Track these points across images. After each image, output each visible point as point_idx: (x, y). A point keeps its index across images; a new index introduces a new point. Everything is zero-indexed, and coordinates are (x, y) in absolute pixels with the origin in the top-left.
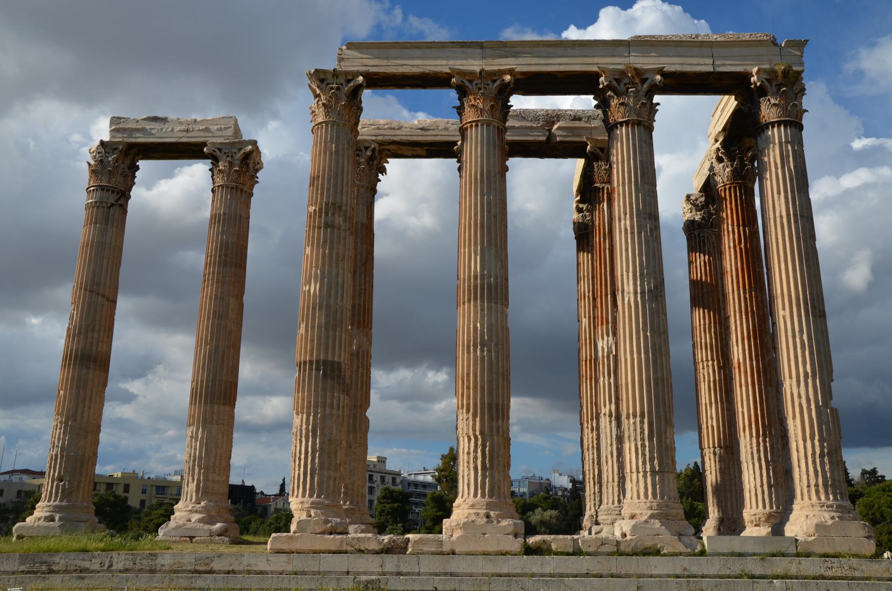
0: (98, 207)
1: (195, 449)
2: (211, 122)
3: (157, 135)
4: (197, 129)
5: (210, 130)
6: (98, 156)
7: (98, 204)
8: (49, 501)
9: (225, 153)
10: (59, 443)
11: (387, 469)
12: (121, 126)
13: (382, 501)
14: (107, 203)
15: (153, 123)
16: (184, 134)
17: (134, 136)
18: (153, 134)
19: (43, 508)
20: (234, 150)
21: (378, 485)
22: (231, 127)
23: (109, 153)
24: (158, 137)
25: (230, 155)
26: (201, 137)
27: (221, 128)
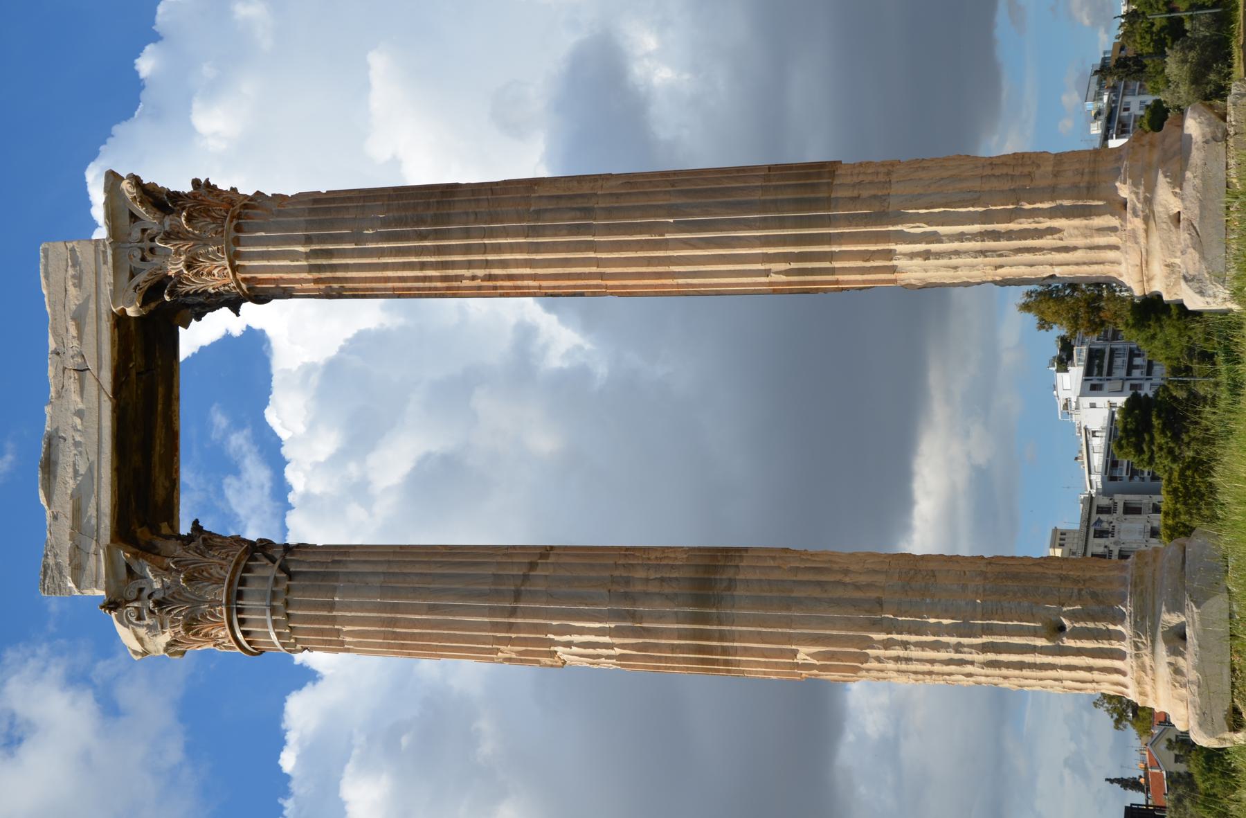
0: (287, 604)
1: (961, 237)
2: (59, 308)
3: (93, 457)
4: (75, 343)
5: (79, 306)
6: (148, 621)
7: (278, 603)
8: (1121, 655)
9: (143, 259)
10: (946, 646)
11: (1077, 527)
12: (65, 561)
13: (1146, 457)
14: (276, 580)
15: (60, 471)
16: (89, 377)
17: (94, 521)
18: (90, 469)
19: (1142, 668)
20: (137, 234)
21: (1116, 543)
22: (73, 250)
23: (141, 590)
24: (99, 453)
25: (147, 244)
26: (98, 332)
27: (73, 277)
